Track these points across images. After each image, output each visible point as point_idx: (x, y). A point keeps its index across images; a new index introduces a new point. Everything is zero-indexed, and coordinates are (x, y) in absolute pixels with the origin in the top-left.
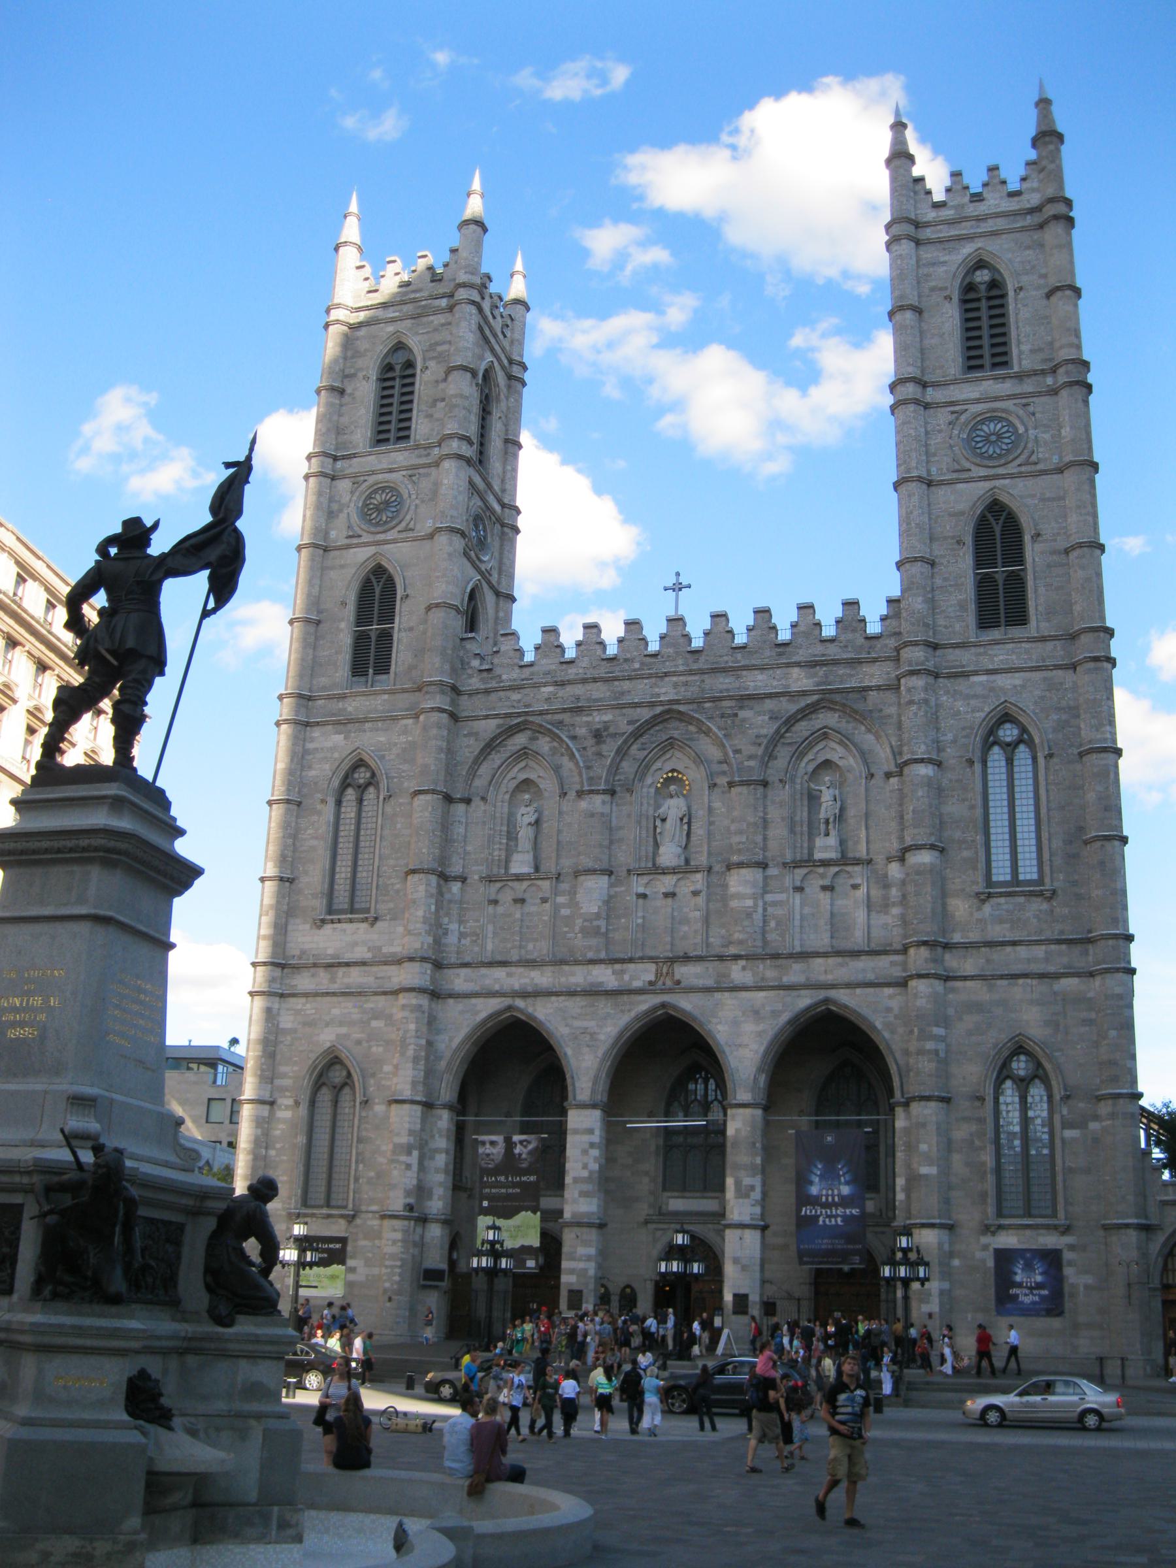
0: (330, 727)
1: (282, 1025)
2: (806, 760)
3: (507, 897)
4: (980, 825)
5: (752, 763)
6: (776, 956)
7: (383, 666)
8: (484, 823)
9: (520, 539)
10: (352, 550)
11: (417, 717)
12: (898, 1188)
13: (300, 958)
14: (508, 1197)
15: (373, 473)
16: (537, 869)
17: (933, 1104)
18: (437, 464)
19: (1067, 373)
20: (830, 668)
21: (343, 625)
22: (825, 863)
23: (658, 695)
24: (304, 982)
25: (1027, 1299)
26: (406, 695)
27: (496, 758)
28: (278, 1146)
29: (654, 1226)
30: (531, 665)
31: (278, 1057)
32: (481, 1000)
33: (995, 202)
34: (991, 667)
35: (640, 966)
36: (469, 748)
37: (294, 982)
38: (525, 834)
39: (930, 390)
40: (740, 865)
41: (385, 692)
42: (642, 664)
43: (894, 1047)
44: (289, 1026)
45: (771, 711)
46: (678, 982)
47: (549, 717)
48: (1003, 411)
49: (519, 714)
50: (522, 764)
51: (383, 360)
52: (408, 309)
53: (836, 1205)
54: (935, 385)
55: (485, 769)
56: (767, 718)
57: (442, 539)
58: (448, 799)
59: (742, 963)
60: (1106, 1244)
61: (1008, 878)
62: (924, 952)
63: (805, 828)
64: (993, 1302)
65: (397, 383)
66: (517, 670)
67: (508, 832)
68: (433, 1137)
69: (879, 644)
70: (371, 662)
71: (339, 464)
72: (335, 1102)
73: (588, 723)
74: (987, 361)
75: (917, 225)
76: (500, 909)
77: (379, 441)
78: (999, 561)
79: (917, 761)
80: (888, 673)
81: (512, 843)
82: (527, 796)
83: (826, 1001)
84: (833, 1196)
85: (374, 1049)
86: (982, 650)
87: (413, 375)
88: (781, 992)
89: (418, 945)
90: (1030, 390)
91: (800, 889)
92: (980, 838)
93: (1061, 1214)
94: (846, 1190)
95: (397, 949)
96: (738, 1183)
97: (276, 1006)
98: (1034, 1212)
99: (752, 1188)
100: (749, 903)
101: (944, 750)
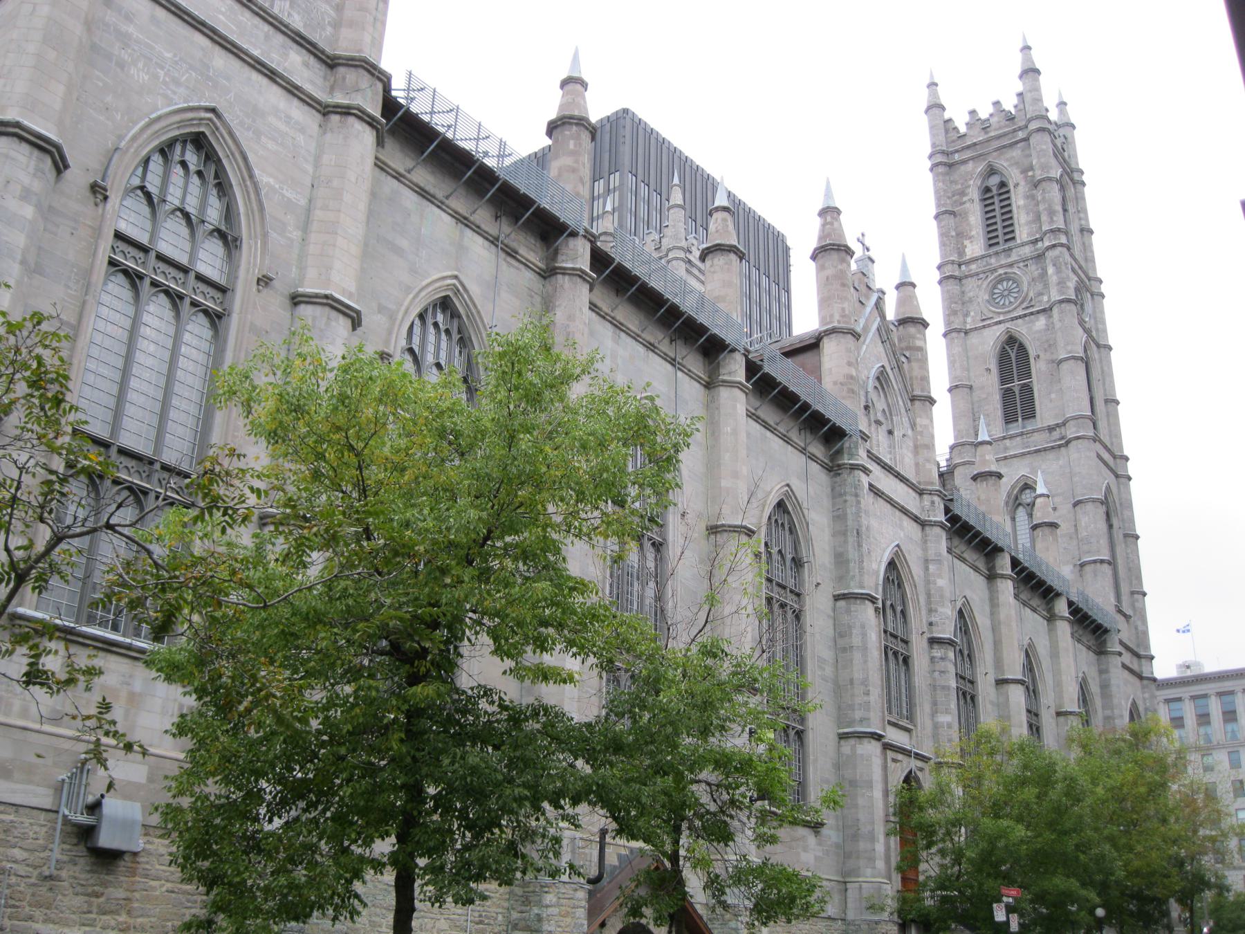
7: (1030, 413)
9: (1107, 303)
70: (1019, 412)
77: (991, 245)
87: (1008, 192)
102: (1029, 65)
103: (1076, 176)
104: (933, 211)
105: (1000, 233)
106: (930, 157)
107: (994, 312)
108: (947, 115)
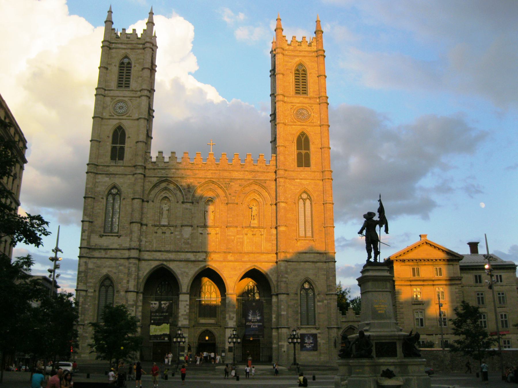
0: (104, 175)
1: (89, 267)
2: (248, 198)
3: (160, 231)
4: (297, 221)
5: (234, 198)
6: (241, 253)
7: (121, 158)
8: (153, 209)
10: (111, 120)
11: (134, 175)
12: (273, 318)
13: (95, 246)
14: (159, 319)
15: (118, 96)
16: (168, 223)
17: (285, 295)
18: (140, 97)
19: (323, 99)
20: (256, 173)
21: (108, 143)
22: (253, 228)
23: (207, 176)
24: (97, 254)
25: (308, 347)
26: (129, 168)
27: (157, 190)
28: (89, 304)
29: (196, 327)
30: (168, 162)
31: (88, 277)
32: (153, 261)
33: (304, 47)
34: (301, 178)
35: (201, 254)
36: (148, 186)
37: (93, 254)
38: (165, 213)
39: (286, 98)
40: (230, 227)
41: (122, 166)
42: (202, 166)
43: (273, 279)
45: (240, 184)
47: (174, 179)
48: (306, 107)
49: (164, 177)
50: (164, 192)
51: (120, 61)
52: (129, 46)
53: (256, 322)
54: (287, 97)
55: (153, 193)
56: (238, 185)
57: (142, 121)
58: (143, 201)
59: (231, 254)
60: (328, 332)
61: (304, 235)
62: (283, 254)
63: (248, 217)
64: (300, 347)
65: (125, 69)
66: (163, 163)
67: (160, 212)
68: (138, 302)
69: (269, 168)
71: (106, 92)
72: (107, 291)
73: (186, 182)
74: (302, 92)
75: (283, 49)
76: (158, 235)
77: (119, 86)
78: (303, 150)
79: (281, 202)
80: (272, 176)
81: (161, 215)
82: (166, 202)
83: (255, 266)
84: (255, 320)
85: (120, 275)
86: (298, 173)
87: (131, 67)
88: (242, 263)
89: (135, 245)
90: (313, 102)
91: (246, 234)
92: (297, 224)
93: (317, 325)
94: (258, 318)
95: (127, 245)
96: (230, 316)
98: (310, 324)
99: (234, 317)
100: (233, 238)
101: (288, 199)
102: (150, 21)
103: (154, 67)
104: (99, 65)
105: (124, 82)
106: (103, 42)
107: (115, 114)
108: (113, 27)
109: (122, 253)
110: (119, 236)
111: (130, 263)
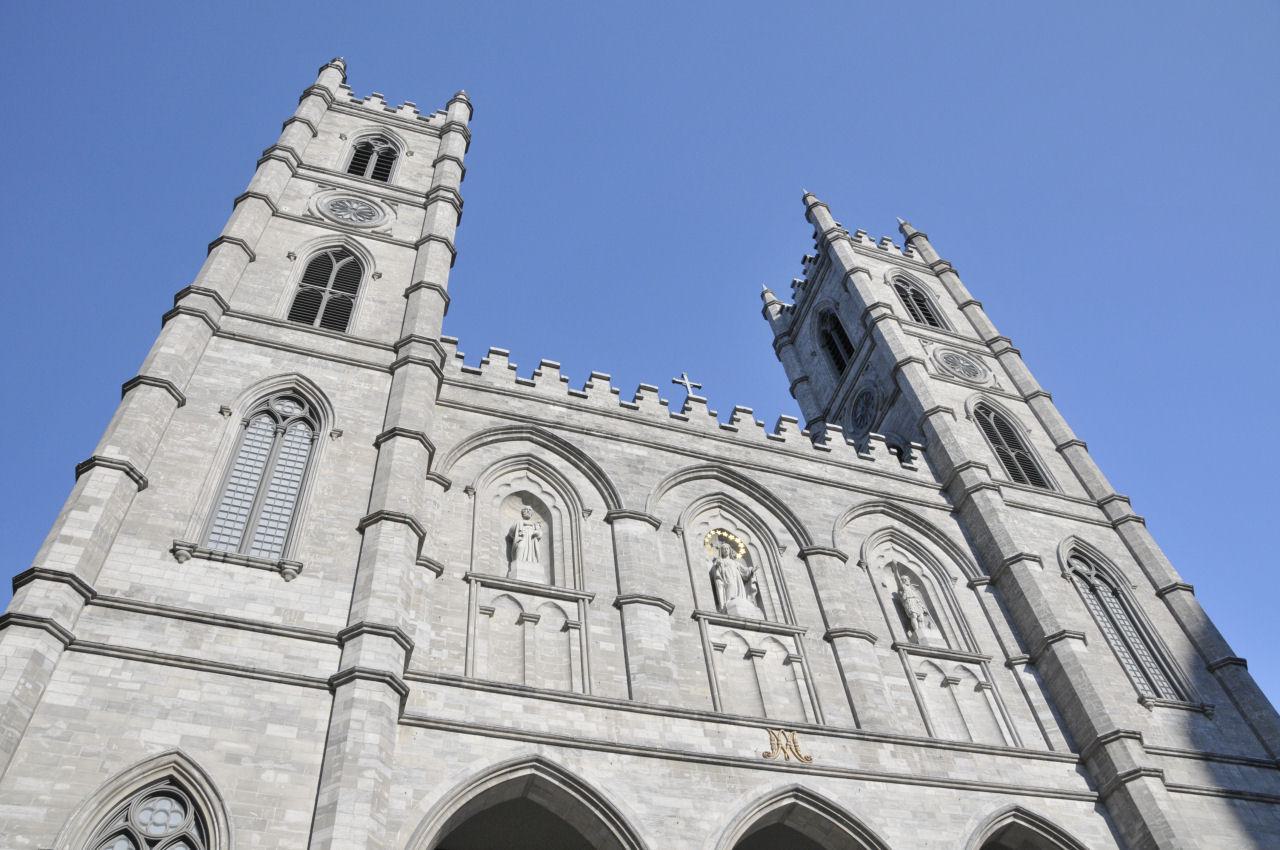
7: (338, 319)
44: (71, 702)
46: (808, 759)
50: (523, 473)
56: (829, 501)
85: (268, 776)
97: (52, 656)
100: (873, 677)
109: (293, 653)
110: (289, 569)
111: (350, 704)
